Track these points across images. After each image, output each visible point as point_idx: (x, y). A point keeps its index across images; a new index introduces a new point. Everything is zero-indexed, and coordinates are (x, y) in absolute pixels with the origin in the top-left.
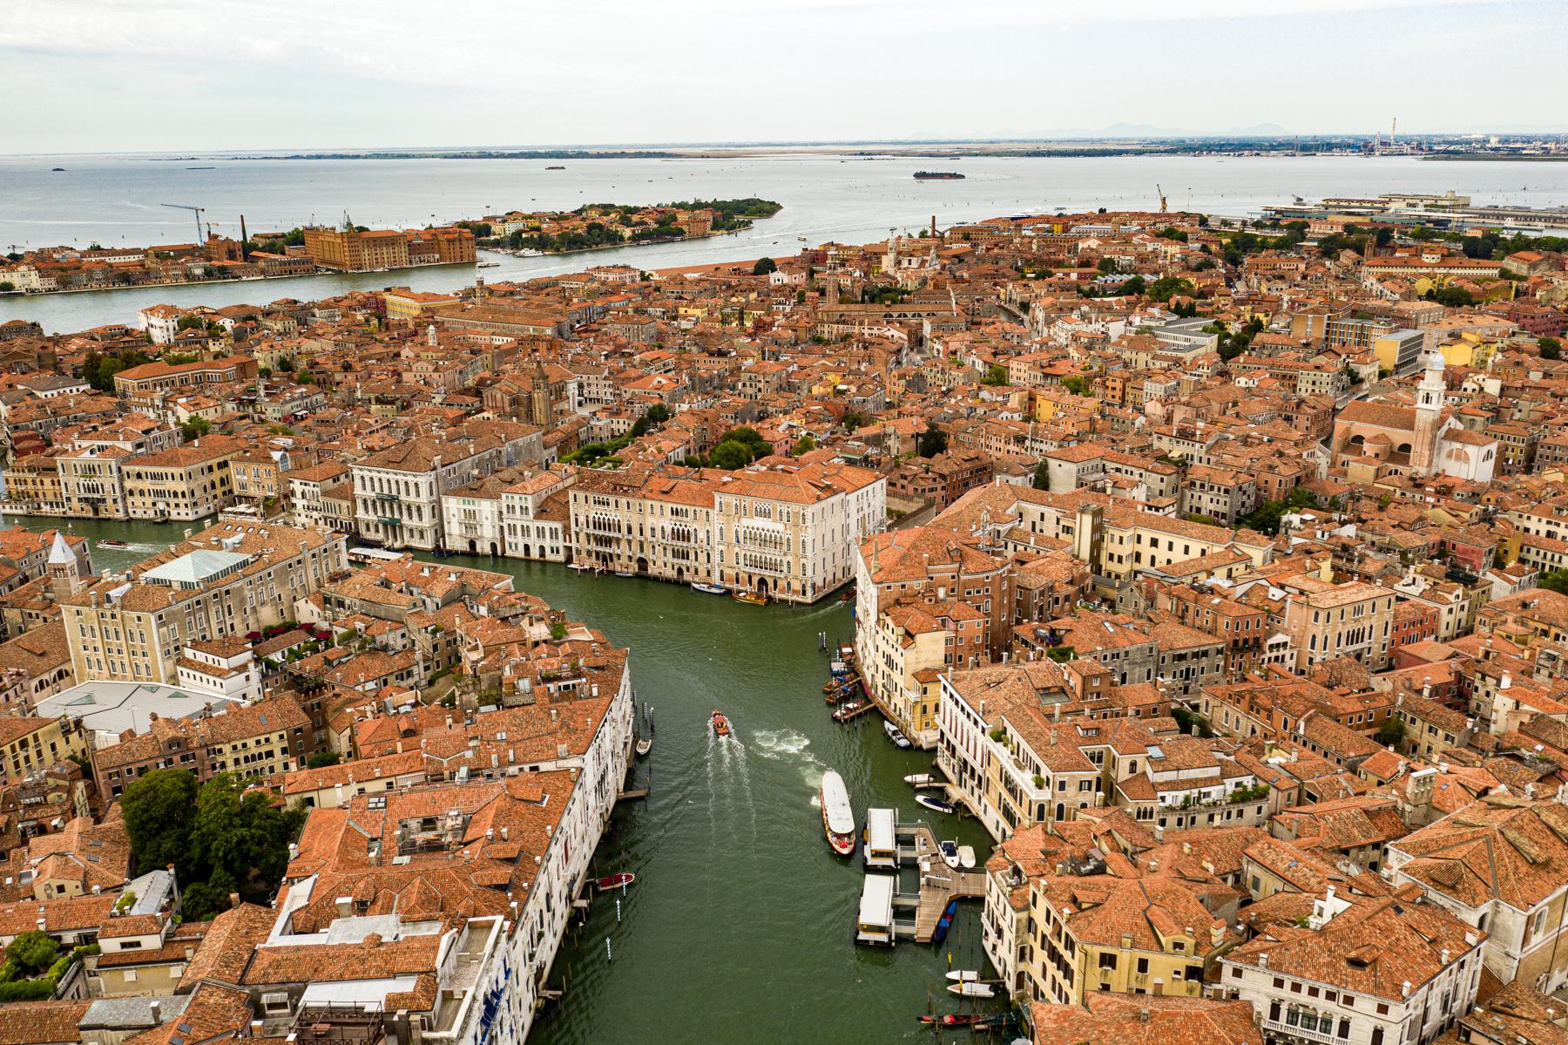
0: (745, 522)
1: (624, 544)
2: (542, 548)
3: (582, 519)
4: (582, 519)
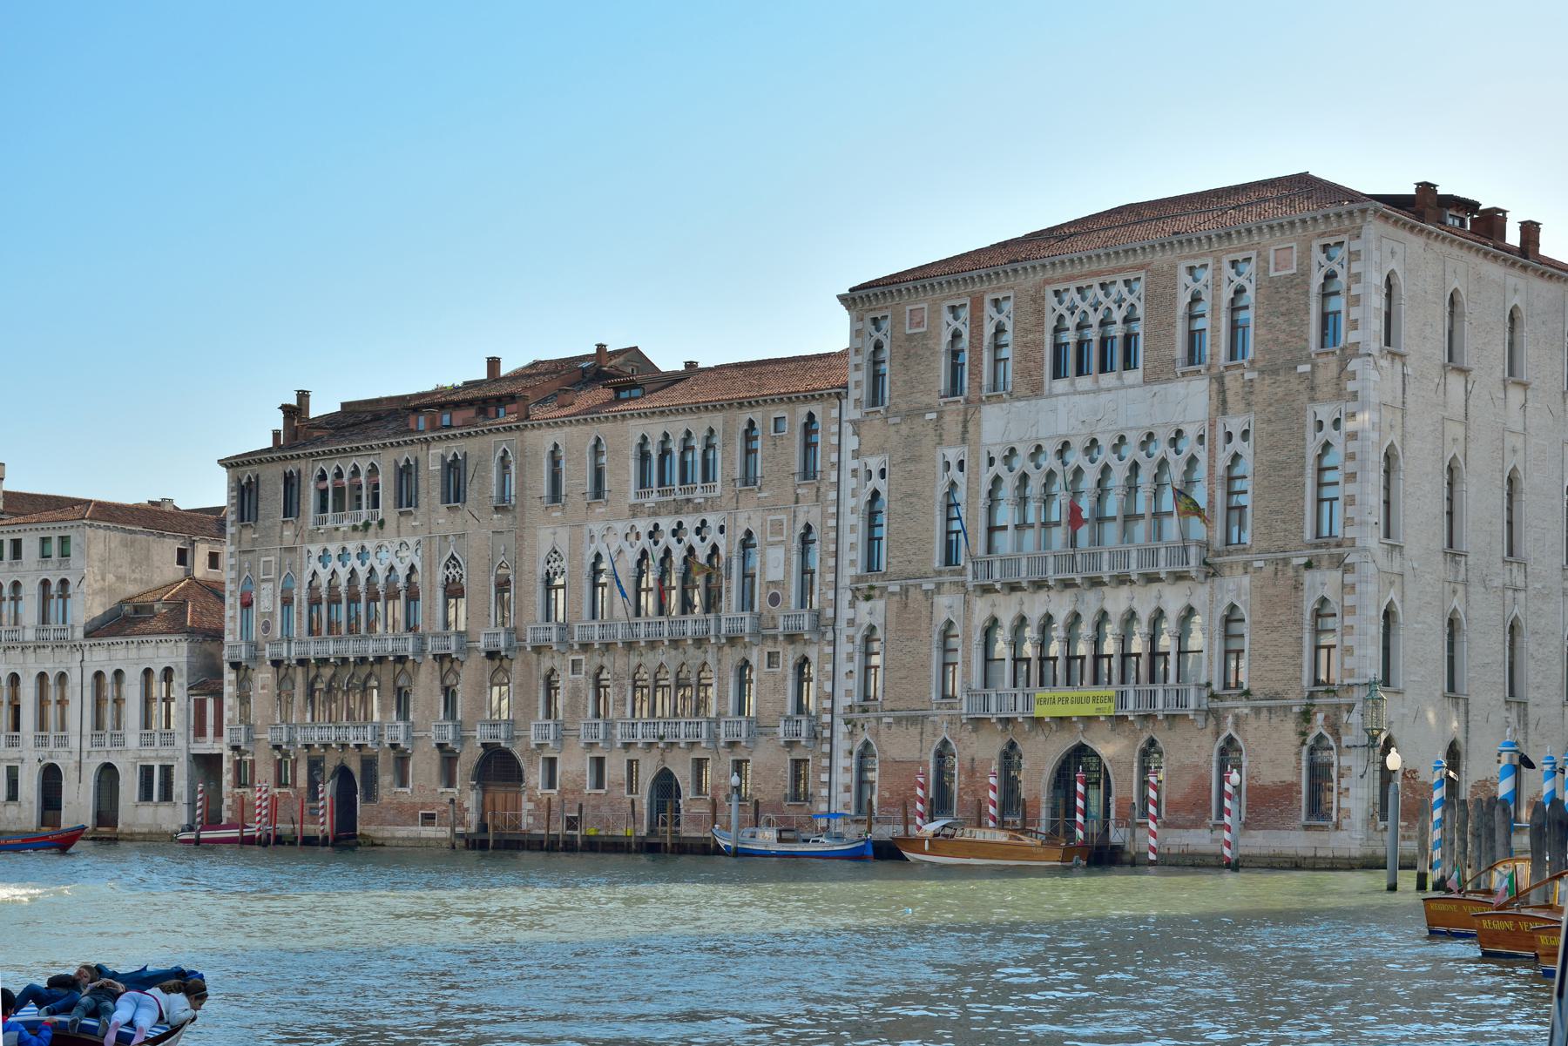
0: (998, 425)
1: (425, 687)
2: (108, 774)
3: (267, 600)
4: (267, 600)
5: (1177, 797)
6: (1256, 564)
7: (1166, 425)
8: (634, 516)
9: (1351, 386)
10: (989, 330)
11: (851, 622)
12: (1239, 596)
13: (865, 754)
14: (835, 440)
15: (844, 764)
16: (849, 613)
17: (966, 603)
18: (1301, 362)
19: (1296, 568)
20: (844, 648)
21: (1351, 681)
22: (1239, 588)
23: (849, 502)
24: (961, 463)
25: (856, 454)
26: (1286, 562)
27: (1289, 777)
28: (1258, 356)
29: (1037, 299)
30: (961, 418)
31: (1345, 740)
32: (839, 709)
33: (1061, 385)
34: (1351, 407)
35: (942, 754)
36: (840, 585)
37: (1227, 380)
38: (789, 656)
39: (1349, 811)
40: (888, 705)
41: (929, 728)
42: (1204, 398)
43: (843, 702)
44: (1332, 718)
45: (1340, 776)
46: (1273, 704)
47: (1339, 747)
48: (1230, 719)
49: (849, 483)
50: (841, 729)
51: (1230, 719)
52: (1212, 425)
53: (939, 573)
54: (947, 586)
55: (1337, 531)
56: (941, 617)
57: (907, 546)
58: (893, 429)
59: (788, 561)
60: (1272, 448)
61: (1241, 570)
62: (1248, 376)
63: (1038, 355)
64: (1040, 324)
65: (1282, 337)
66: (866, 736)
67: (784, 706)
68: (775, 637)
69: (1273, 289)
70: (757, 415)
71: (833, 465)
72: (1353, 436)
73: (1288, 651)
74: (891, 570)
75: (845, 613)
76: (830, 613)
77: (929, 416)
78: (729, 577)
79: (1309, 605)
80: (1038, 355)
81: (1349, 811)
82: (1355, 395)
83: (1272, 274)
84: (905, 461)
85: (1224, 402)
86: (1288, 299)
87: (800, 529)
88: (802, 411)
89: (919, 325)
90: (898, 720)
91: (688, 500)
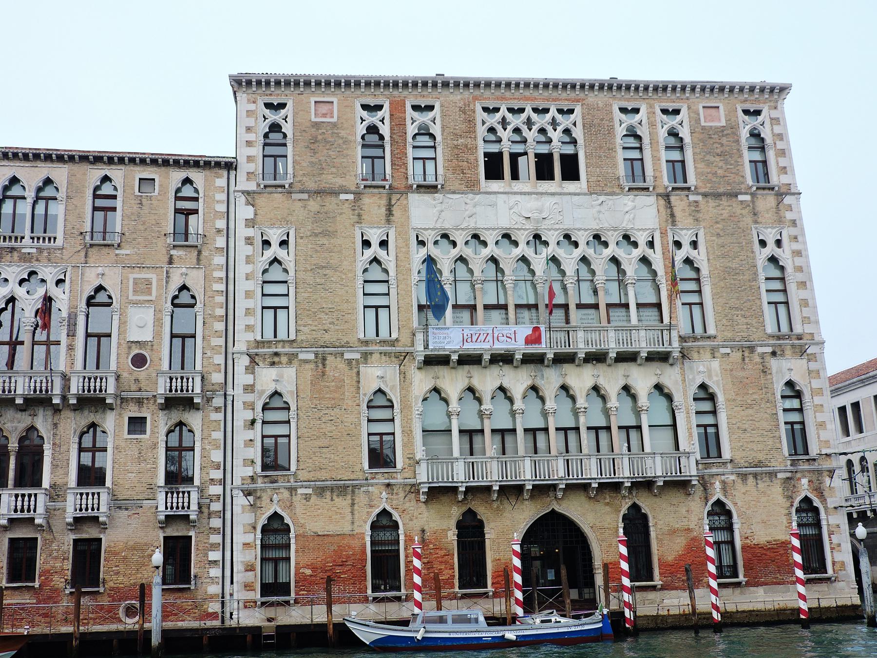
0: (423, 213)
5: (670, 558)
6: (724, 351)
7: (615, 229)
9: (789, 216)
10: (411, 130)
11: (249, 389)
12: (710, 376)
13: (275, 529)
14: (222, 208)
16: (249, 379)
17: (403, 375)
18: (741, 193)
19: (762, 356)
20: (242, 415)
21: (828, 451)
22: (709, 371)
23: (243, 269)
24: (384, 244)
25: (250, 223)
26: (752, 349)
27: (782, 537)
28: (700, 184)
29: (467, 112)
30: (384, 202)
31: (831, 502)
33: (495, 185)
34: (793, 231)
35: (384, 523)
36: (230, 350)
37: (673, 199)
38: (159, 425)
39: (843, 563)
40: (302, 475)
41: (361, 498)
42: (653, 211)
43: (242, 472)
44: (816, 483)
45: (831, 534)
46: (756, 472)
47: (826, 508)
48: (718, 485)
49: (243, 250)
50: (241, 501)
51: (718, 485)
52: (663, 234)
53: (366, 343)
54: (376, 356)
55: (798, 329)
56: (370, 385)
57: (322, 316)
58: (300, 204)
59: (158, 322)
60: (724, 256)
61: (708, 355)
62: (692, 198)
63: (472, 158)
64: (471, 130)
65: (720, 172)
67: (155, 475)
68: (139, 402)
69: (705, 135)
70: (117, 173)
71: (219, 231)
72: (798, 253)
73: (765, 425)
74: (300, 338)
75: (242, 378)
76: (217, 378)
77: (343, 197)
78: (71, 334)
79: (779, 387)
80: (472, 158)
81: (843, 563)
82: (794, 223)
83: (703, 124)
84: (316, 235)
85: (672, 215)
86: (722, 145)
87: (173, 289)
88: (177, 176)
89: (324, 115)
90: (320, 491)
91: (13, 249)
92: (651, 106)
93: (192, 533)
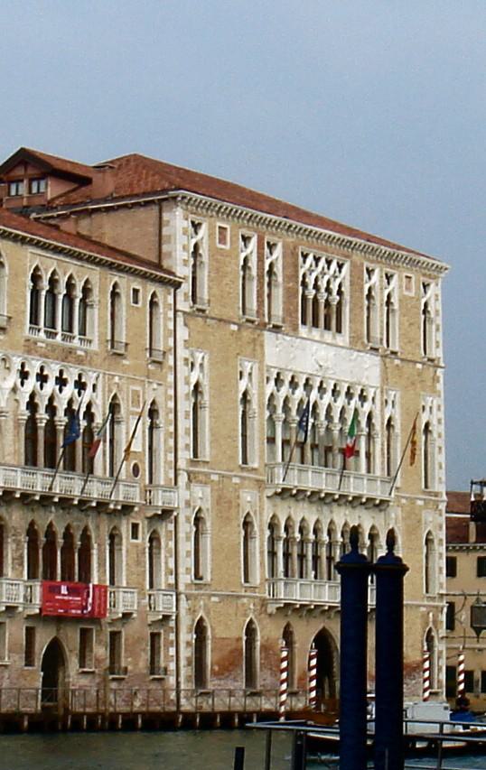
8: (29, 352)
15: (187, 636)
32: (181, 588)
66: (201, 613)
92: (381, 270)
93: (162, 631)
